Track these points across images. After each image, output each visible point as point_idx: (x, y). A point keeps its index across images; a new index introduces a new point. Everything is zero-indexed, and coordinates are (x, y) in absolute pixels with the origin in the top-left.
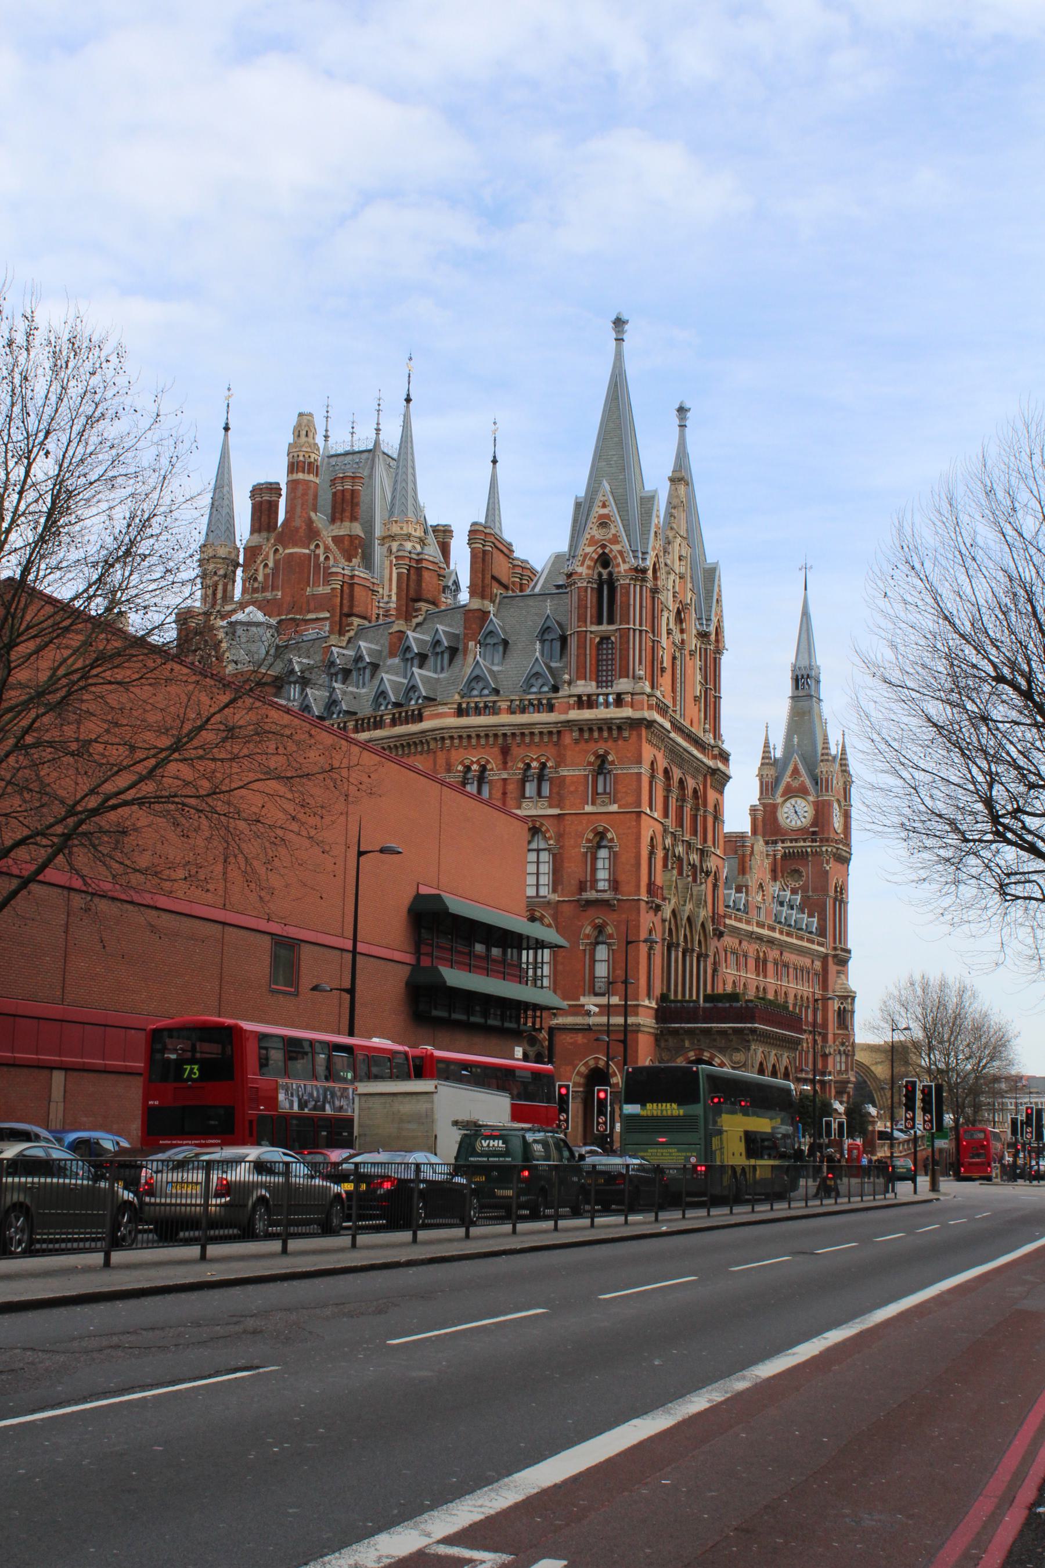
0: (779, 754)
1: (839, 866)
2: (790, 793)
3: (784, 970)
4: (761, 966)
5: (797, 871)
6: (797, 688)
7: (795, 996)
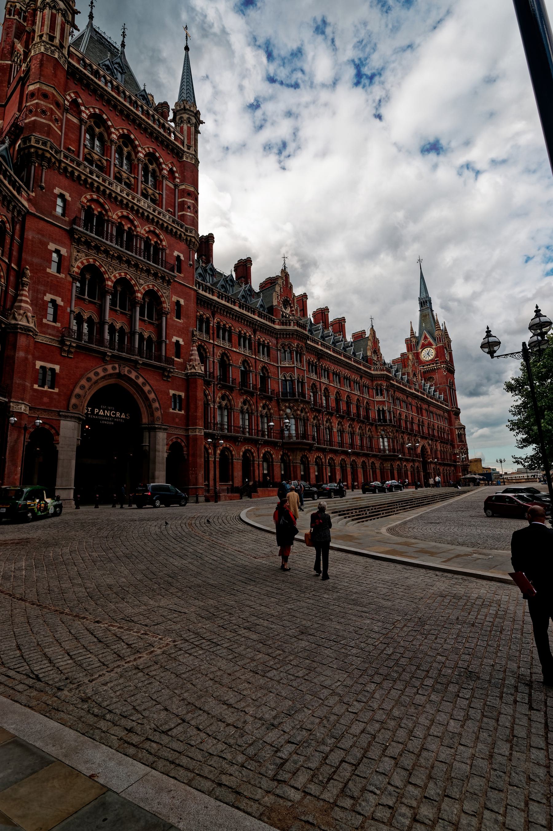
0: (417, 335)
1: (450, 374)
2: (424, 347)
3: (431, 415)
4: (419, 410)
5: (431, 378)
6: (422, 306)
7: (438, 427)
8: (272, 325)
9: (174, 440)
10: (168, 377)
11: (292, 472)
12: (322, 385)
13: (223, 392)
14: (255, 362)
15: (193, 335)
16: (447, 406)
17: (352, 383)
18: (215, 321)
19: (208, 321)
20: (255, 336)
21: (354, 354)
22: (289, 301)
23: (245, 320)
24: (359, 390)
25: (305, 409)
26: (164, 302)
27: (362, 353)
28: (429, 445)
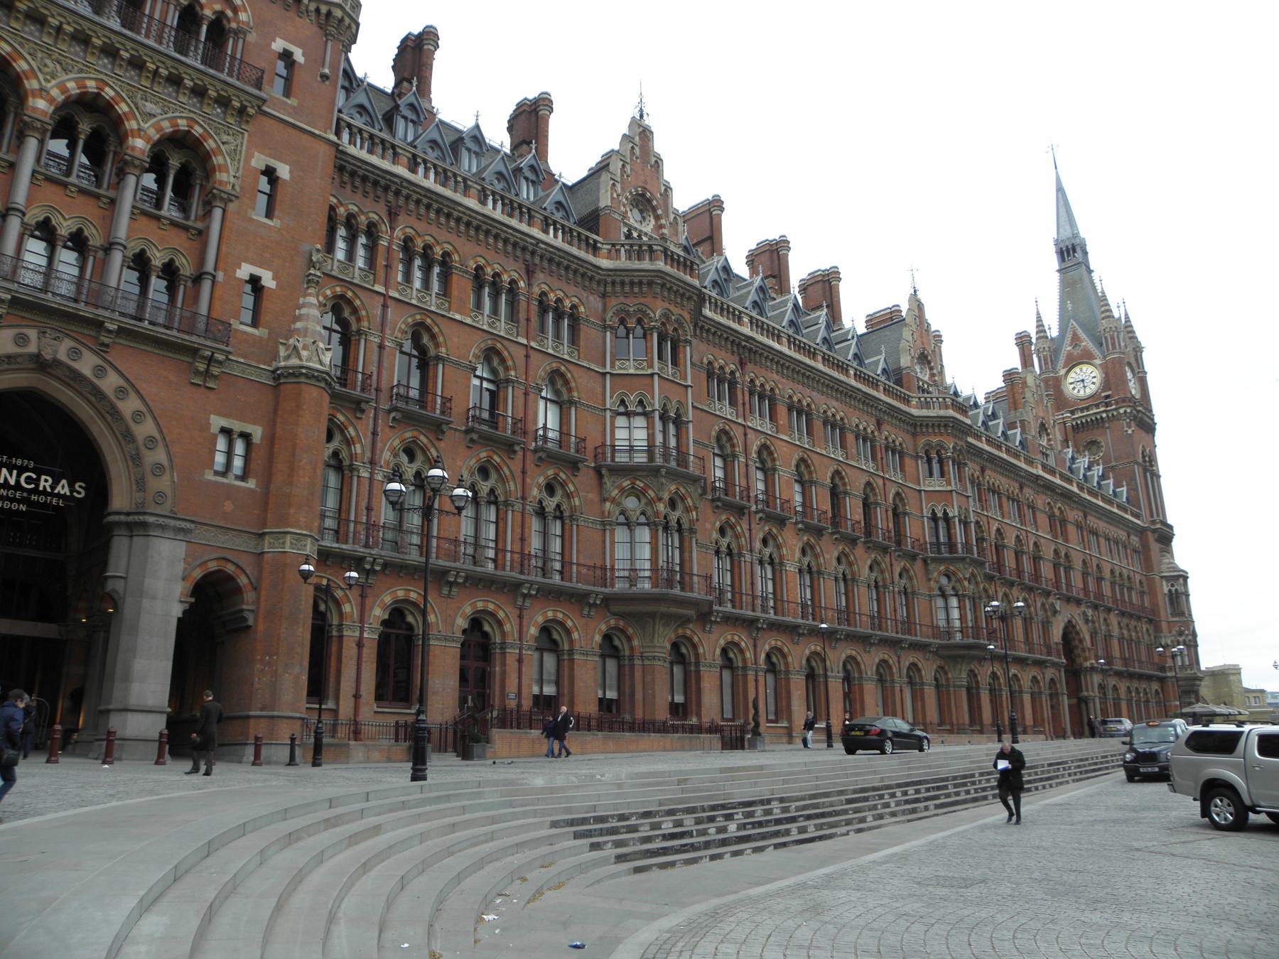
0: (1054, 332)
1: (1144, 434)
2: (1072, 363)
4: (1058, 524)
7: (1112, 572)
8: (590, 258)
9: (213, 566)
10: (207, 374)
11: (639, 687)
12: (751, 435)
13: (408, 435)
14: (527, 356)
15: (311, 264)
16: (1137, 516)
17: (850, 438)
18: (398, 233)
19: (372, 232)
20: (530, 285)
21: (856, 356)
22: (649, 201)
23: (496, 237)
24: (874, 458)
25: (683, 499)
26: (224, 168)
27: (882, 357)
28: (1087, 621)
